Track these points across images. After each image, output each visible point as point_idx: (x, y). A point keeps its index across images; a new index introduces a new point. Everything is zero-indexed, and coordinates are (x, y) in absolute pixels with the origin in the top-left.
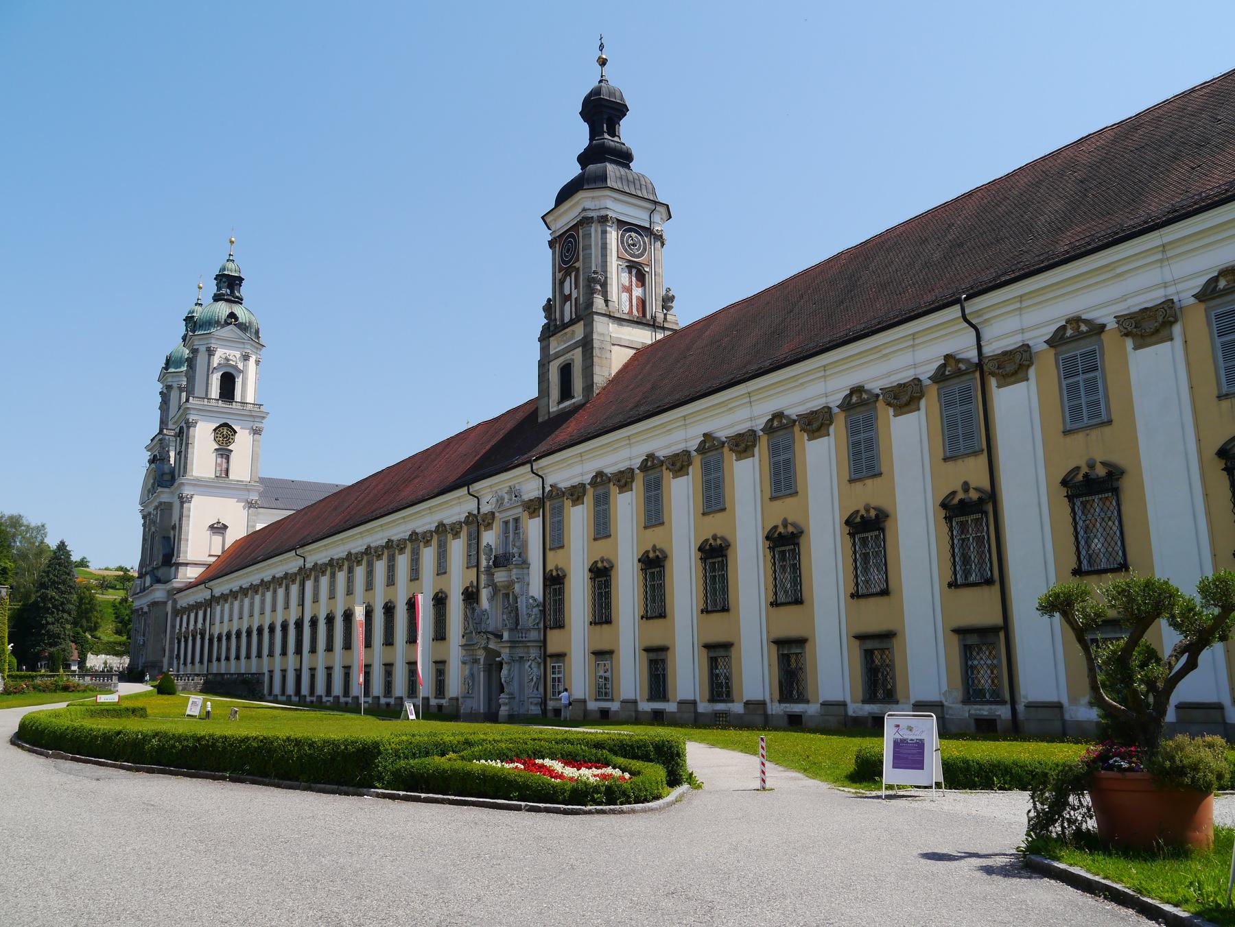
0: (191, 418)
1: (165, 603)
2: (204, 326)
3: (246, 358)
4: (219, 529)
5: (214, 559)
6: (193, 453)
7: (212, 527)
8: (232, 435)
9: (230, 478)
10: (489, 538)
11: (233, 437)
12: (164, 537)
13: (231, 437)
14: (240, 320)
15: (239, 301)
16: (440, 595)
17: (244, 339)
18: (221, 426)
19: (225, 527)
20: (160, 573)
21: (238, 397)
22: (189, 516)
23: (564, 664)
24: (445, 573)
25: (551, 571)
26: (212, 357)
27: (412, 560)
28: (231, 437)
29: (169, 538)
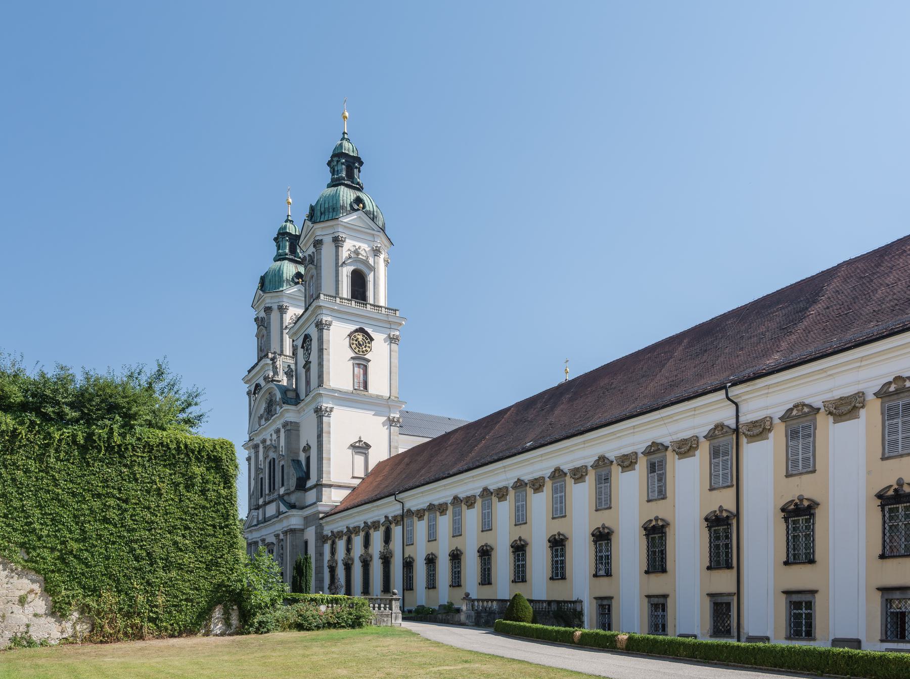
0: (325, 319)
1: (303, 530)
3: (376, 252)
4: (361, 448)
5: (358, 481)
6: (329, 361)
7: (353, 446)
9: (369, 392)
11: (370, 345)
13: (368, 345)
14: (367, 208)
17: (374, 230)
18: (356, 331)
19: (368, 446)
20: (293, 499)
21: (371, 300)
22: (329, 433)
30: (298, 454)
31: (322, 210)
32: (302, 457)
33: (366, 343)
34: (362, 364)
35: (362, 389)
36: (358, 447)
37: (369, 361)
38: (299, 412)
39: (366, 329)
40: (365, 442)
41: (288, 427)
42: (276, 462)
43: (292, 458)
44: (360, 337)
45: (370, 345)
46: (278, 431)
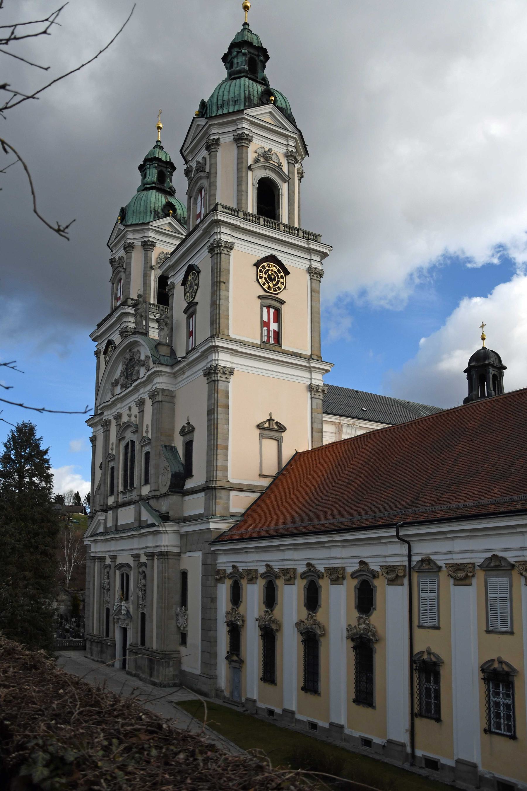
2: (225, 104)
5: (265, 483)
6: (227, 299)
8: (282, 277)
9: (284, 347)
11: (284, 281)
12: (166, 446)
13: (281, 280)
18: (267, 259)
19: (281, 428)
21: (285, 220)
22: (227, 407)
26: (244, 149)
28: (281, 280)
29: (173, 450)
30: (171, 437)
31: (219, 103)
32: (179, 443)
33: (278, 278)
34: (273, 307)
35: (272, 341)
36: (268, 429)
37: (282, 302)
38: (175, 375)
39: (280, 257)
40: (277, 423)
41: (159, 398)
42: (137, 448)
43: (163, 444)
44: (274, 267)
45: (284, 281)
46: (141, 404)
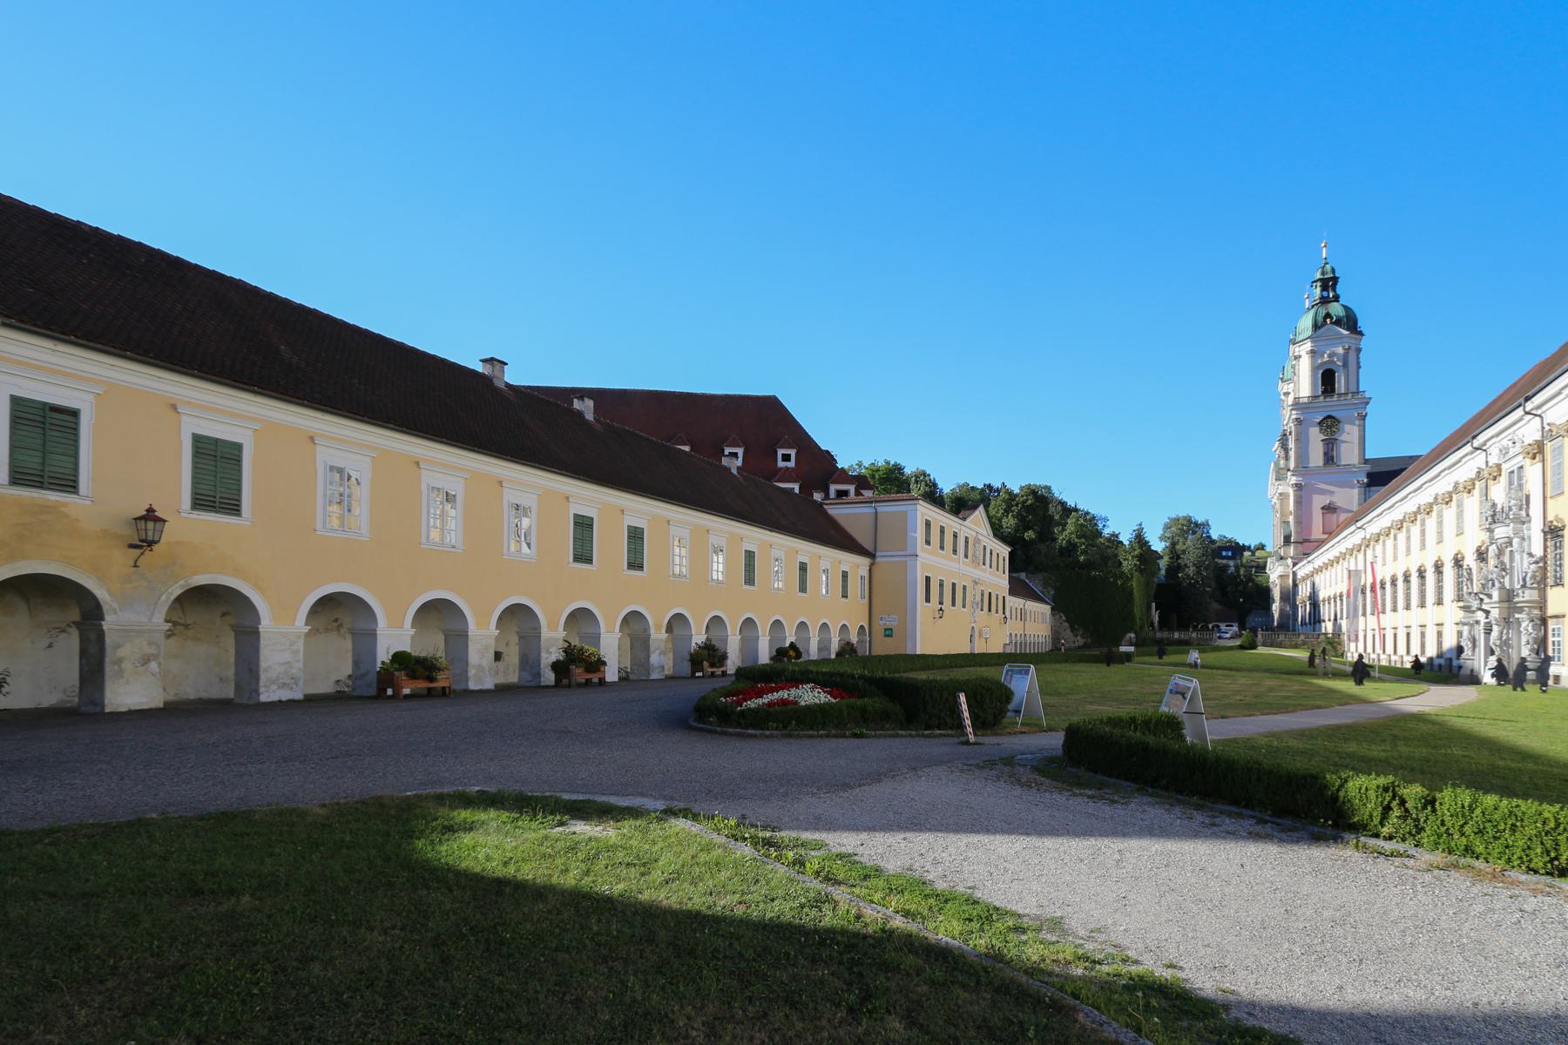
10: (1499, 492)
15: (1336, 299)
16: (1459, 556)
23: (1563, 625)
24: (1462, 534)
25: (1551, 522)
27: (1438, 523)
